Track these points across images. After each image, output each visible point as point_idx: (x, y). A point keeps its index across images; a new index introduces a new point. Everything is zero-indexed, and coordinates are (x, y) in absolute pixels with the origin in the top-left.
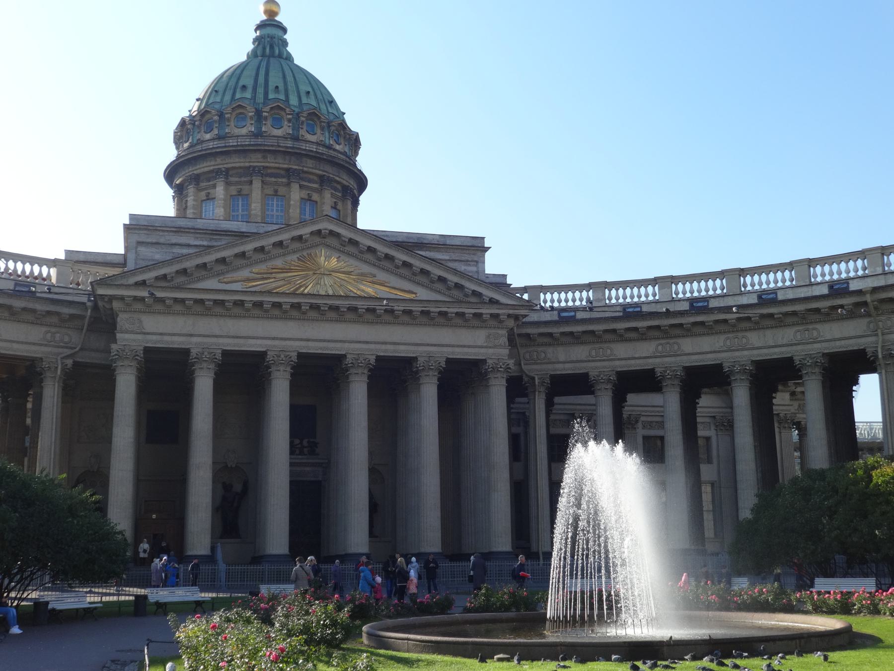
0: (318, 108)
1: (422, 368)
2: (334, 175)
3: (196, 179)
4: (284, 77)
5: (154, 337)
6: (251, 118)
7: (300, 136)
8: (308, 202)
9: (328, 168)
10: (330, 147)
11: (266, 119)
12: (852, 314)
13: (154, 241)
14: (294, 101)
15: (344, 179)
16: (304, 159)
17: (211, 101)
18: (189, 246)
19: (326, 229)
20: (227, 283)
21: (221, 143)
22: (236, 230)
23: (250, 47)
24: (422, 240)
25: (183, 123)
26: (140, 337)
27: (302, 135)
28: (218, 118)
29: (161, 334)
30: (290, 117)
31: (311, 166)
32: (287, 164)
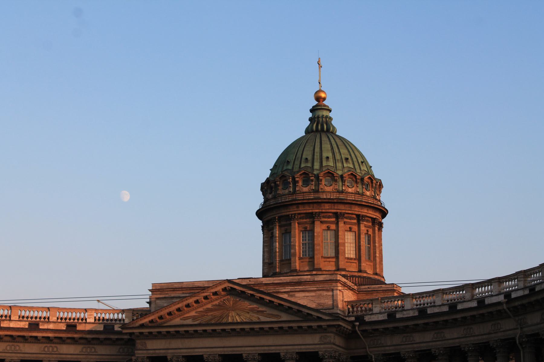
0: (335, 167)
1: (288, 358)
2: (346, 210)
5: (152, 351)
7: (320, 189)
8: (329, 231)
9: (342, 207)
10: (342, 192)
14: (317, 166)
15: (355, 211)
16: (323, 204)
19: (228, 287)
20: (185, 320)
22: (202, 286)
24: (301, 280)
26: (145, 352)
27: (321, 189)
28: (274, 184)
30: (311, 178)
31: (328, 208)
32: (311, 209)
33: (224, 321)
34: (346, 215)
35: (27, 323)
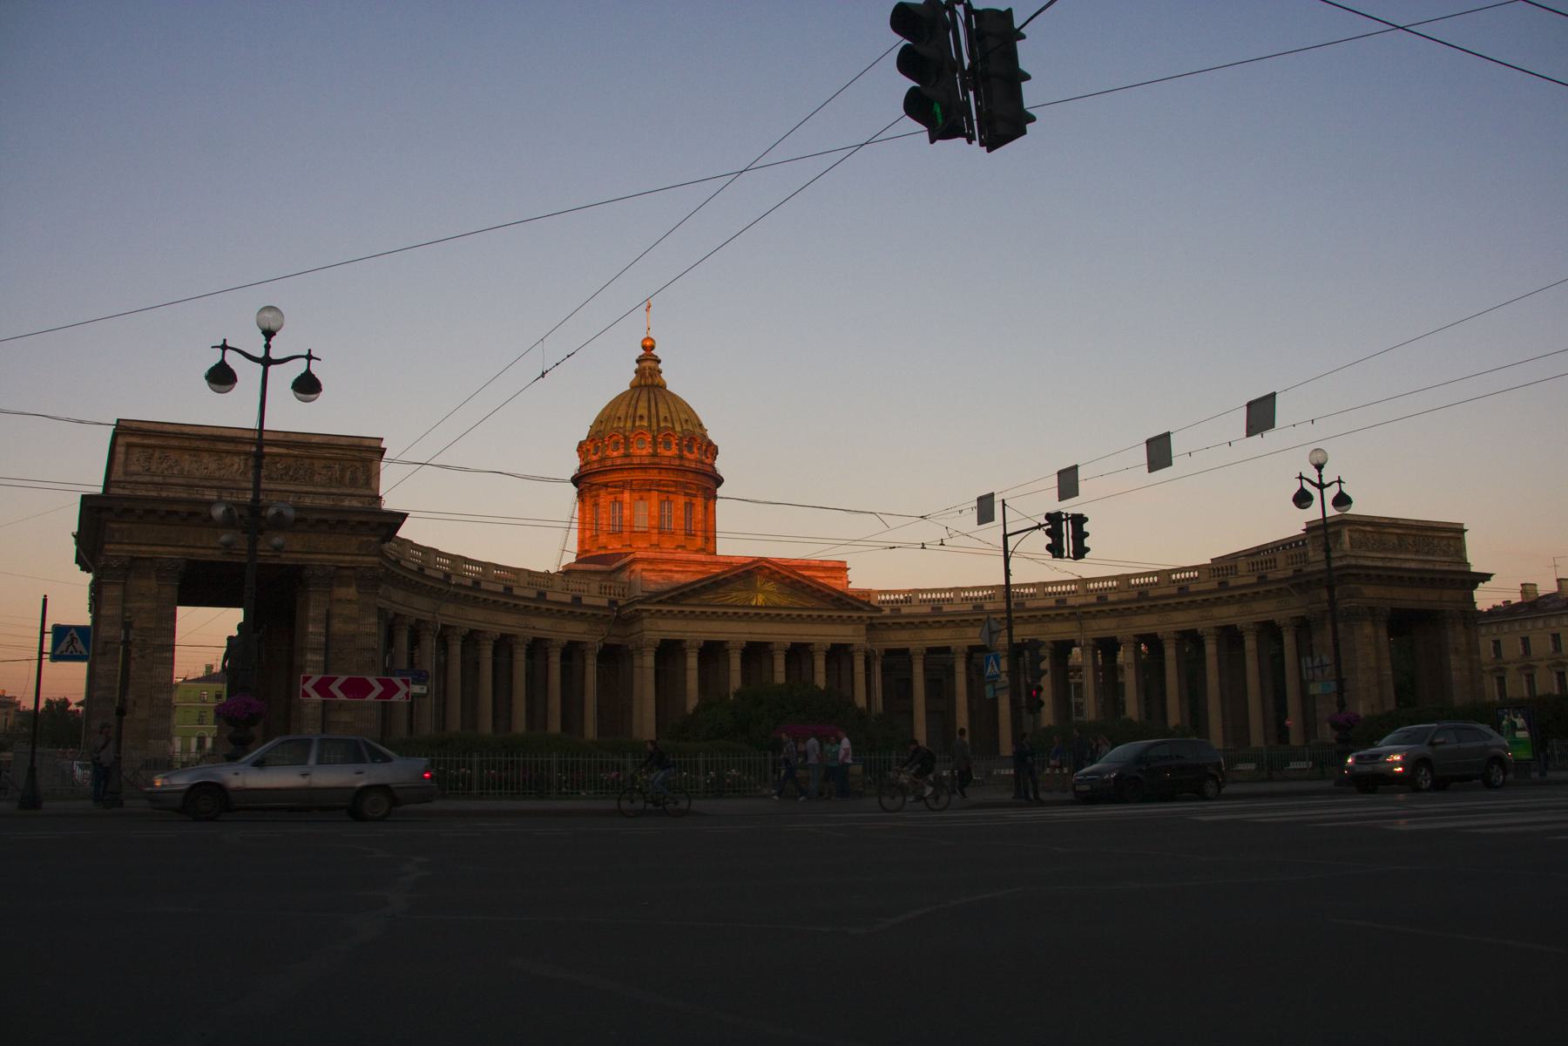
3: (606, 485)
4: (669, 408)
6: (650, 442)
10: (702, 462)
11: (660, 443)
12: (1067, 618)
13: (651, 567)
14: (678, 428)
16: (687, 473)
17: (615, 425)
18: (671, 571)
21: (627, 461)
23: (635, 375)
25: (592, 438)
26: (657, 633)
29: (670, 631)
33: (754, 603)
34: (610, 485)
35: (971, 606)
